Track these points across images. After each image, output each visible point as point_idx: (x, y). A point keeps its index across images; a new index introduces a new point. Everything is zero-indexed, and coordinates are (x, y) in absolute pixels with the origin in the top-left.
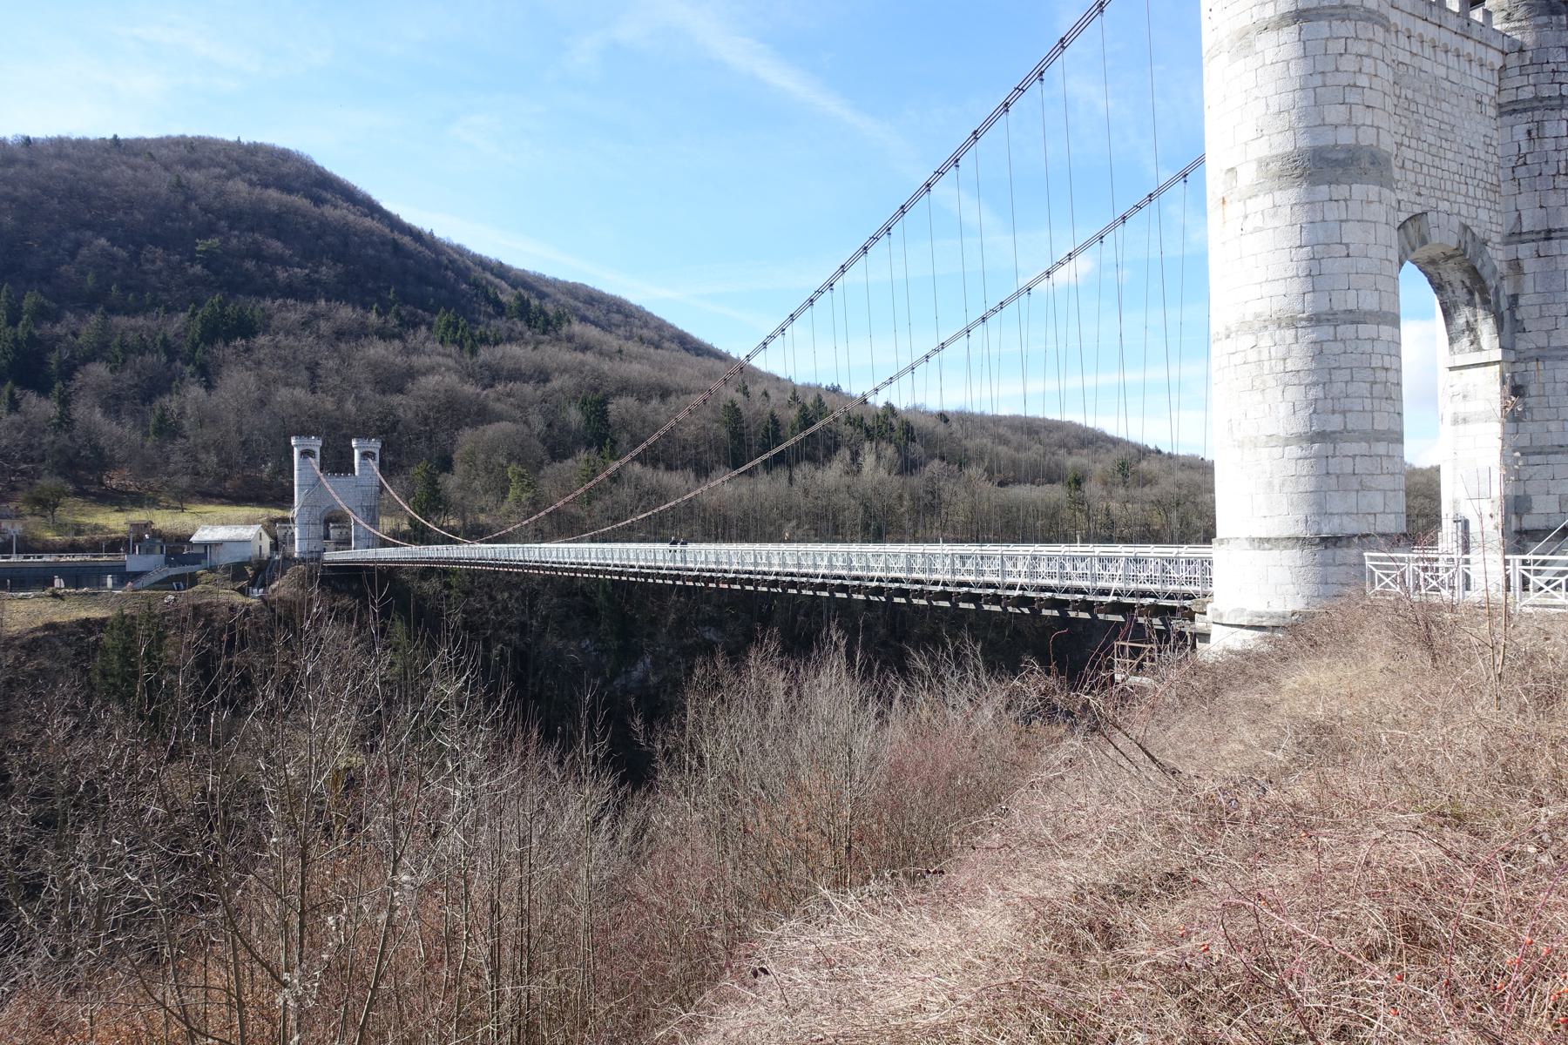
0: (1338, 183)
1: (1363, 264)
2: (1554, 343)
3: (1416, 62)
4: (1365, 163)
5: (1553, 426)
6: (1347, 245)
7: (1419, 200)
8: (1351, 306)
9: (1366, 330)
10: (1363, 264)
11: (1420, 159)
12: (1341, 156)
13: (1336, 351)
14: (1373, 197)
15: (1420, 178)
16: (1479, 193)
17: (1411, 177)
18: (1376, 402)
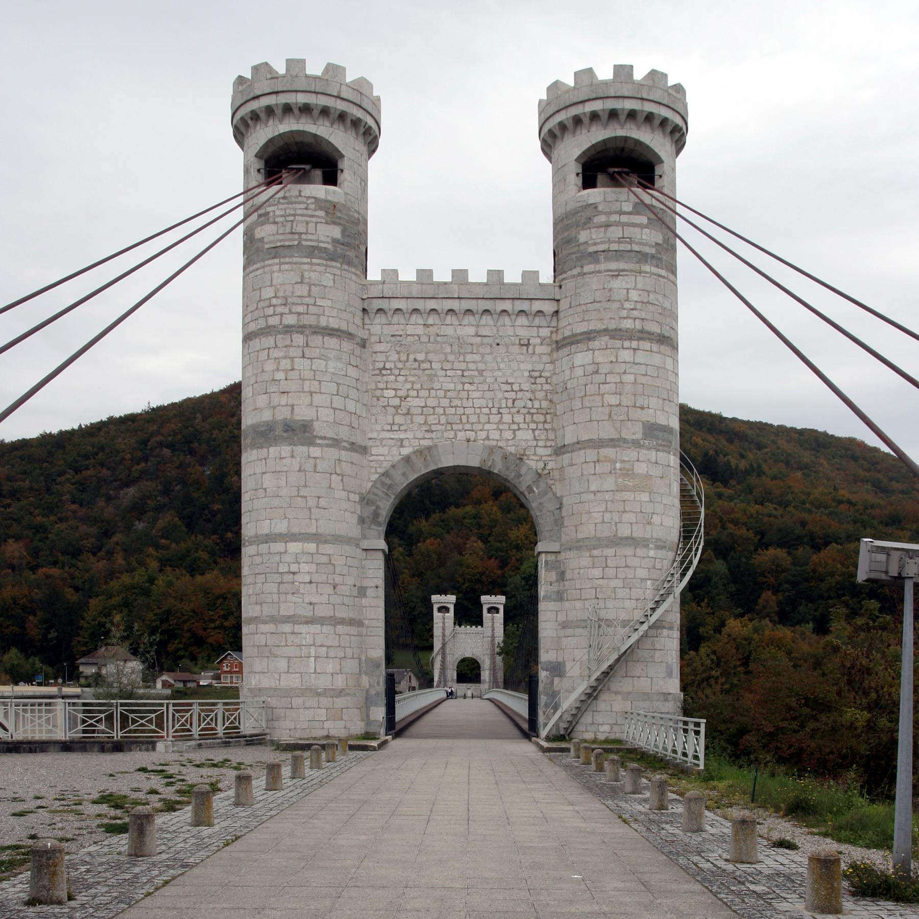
0: (261, 447)
1: (276, 502)
2: (580, 536)
3: (433, 330)
4: (279, 431)
5: (578, 604)
6: (265, 489)
7: (428, 435)
8: (266, 531)
9: (278, 547)
10: (276, 502)
11: (432, 402)
12: (263, 429)
13: (258, 562)
14: (283, 455)
15: (432, 419)
16: (519, 418)
17: (421, 419)
18: (282, 597)
